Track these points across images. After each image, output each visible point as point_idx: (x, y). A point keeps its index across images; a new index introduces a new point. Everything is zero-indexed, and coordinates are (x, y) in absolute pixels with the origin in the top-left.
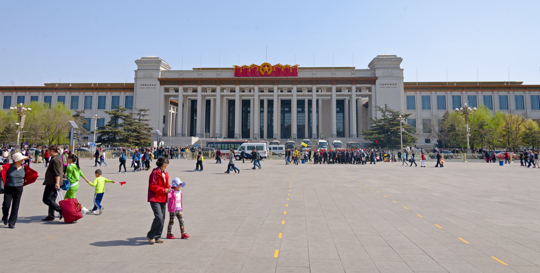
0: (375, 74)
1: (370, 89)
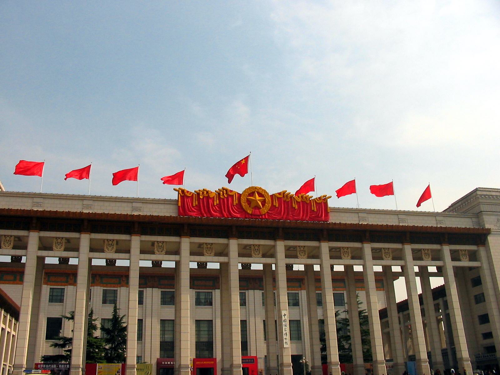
1: (473, 256)
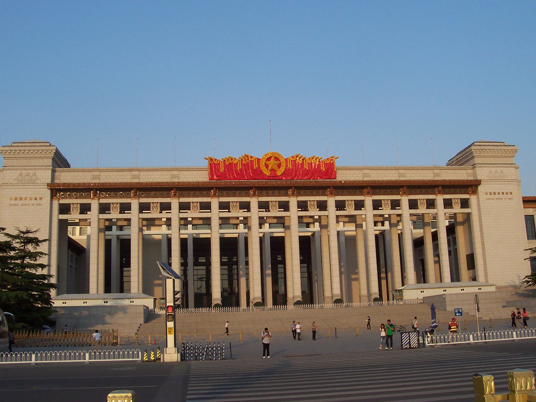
0: (475, 174)
